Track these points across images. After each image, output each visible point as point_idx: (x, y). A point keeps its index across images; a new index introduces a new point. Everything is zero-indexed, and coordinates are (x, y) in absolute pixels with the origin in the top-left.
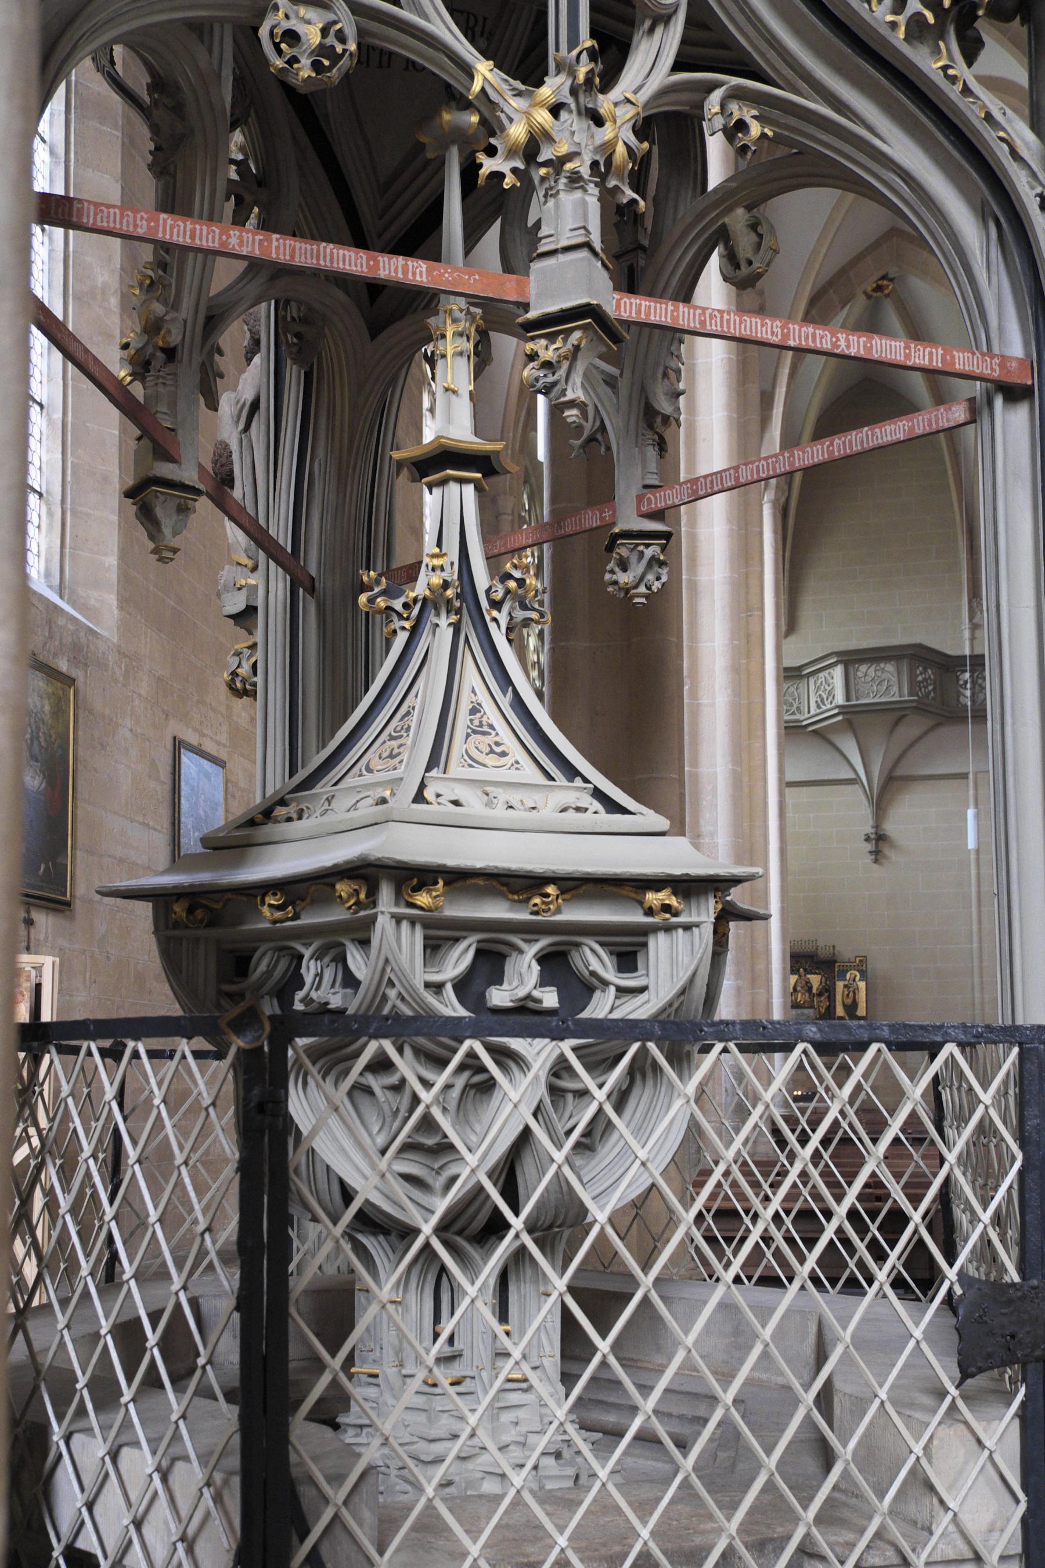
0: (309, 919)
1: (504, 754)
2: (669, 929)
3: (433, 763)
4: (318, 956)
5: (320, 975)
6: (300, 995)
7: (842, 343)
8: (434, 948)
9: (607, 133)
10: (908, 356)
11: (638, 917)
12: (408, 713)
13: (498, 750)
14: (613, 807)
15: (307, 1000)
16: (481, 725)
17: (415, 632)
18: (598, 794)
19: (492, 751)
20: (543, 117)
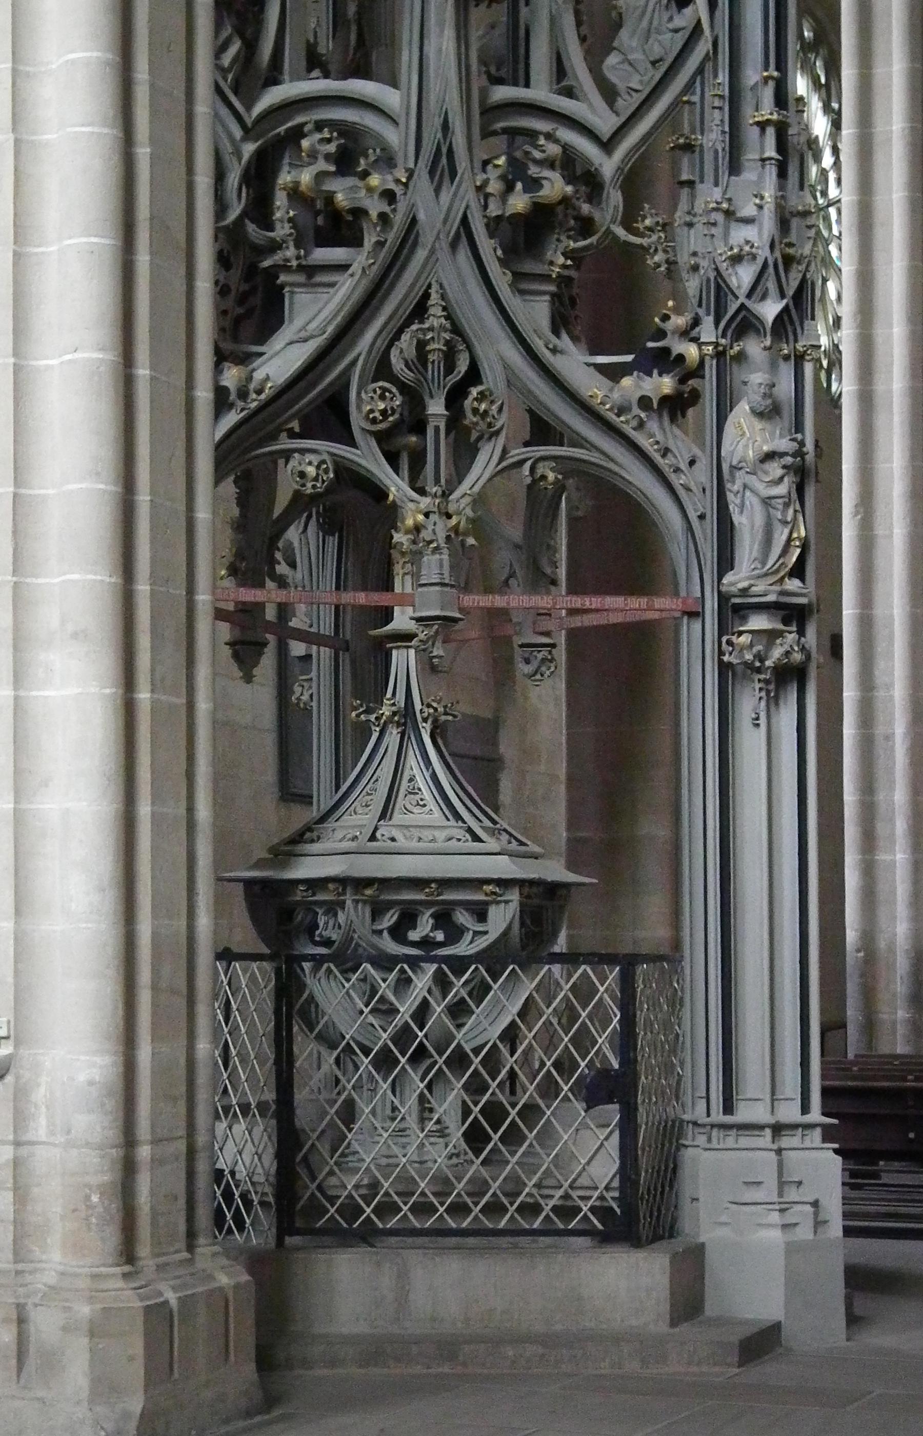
0: (321, 897)
1: (424, 805)
2: (498, 903)
3: (383, 816)
4: (325, 913)
5: (326, 923)
6: (317, 932)
7: (588, 603)
8: (376, 914)
9: (454, 521)
10: (626, 605)
11: (482, 897)
12: (377, 780)
13: (421, 803)
14: (476, 838)
15: (321, 935)
16: (414, 788)
17: (382, 733)
18: (470, 830)
19: (418, 804)
20: (421, 517)
